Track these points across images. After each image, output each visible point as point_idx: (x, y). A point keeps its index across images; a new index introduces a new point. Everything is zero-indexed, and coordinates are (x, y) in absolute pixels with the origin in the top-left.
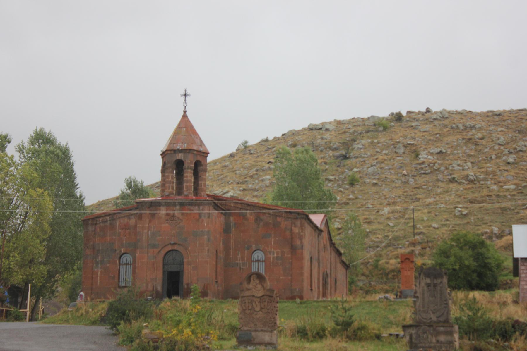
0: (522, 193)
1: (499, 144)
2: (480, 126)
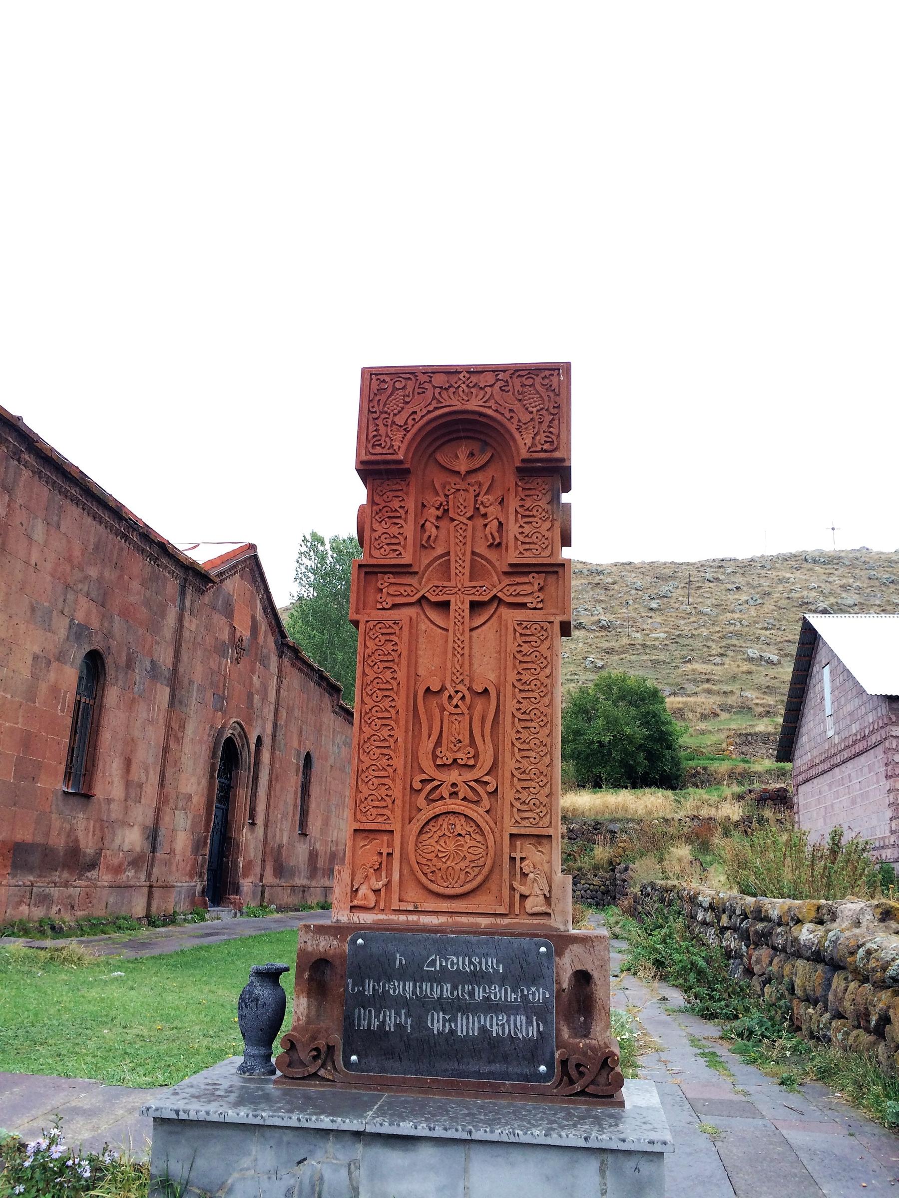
0: (677, 643)
1: (636, 589)
2: (609, 571)
